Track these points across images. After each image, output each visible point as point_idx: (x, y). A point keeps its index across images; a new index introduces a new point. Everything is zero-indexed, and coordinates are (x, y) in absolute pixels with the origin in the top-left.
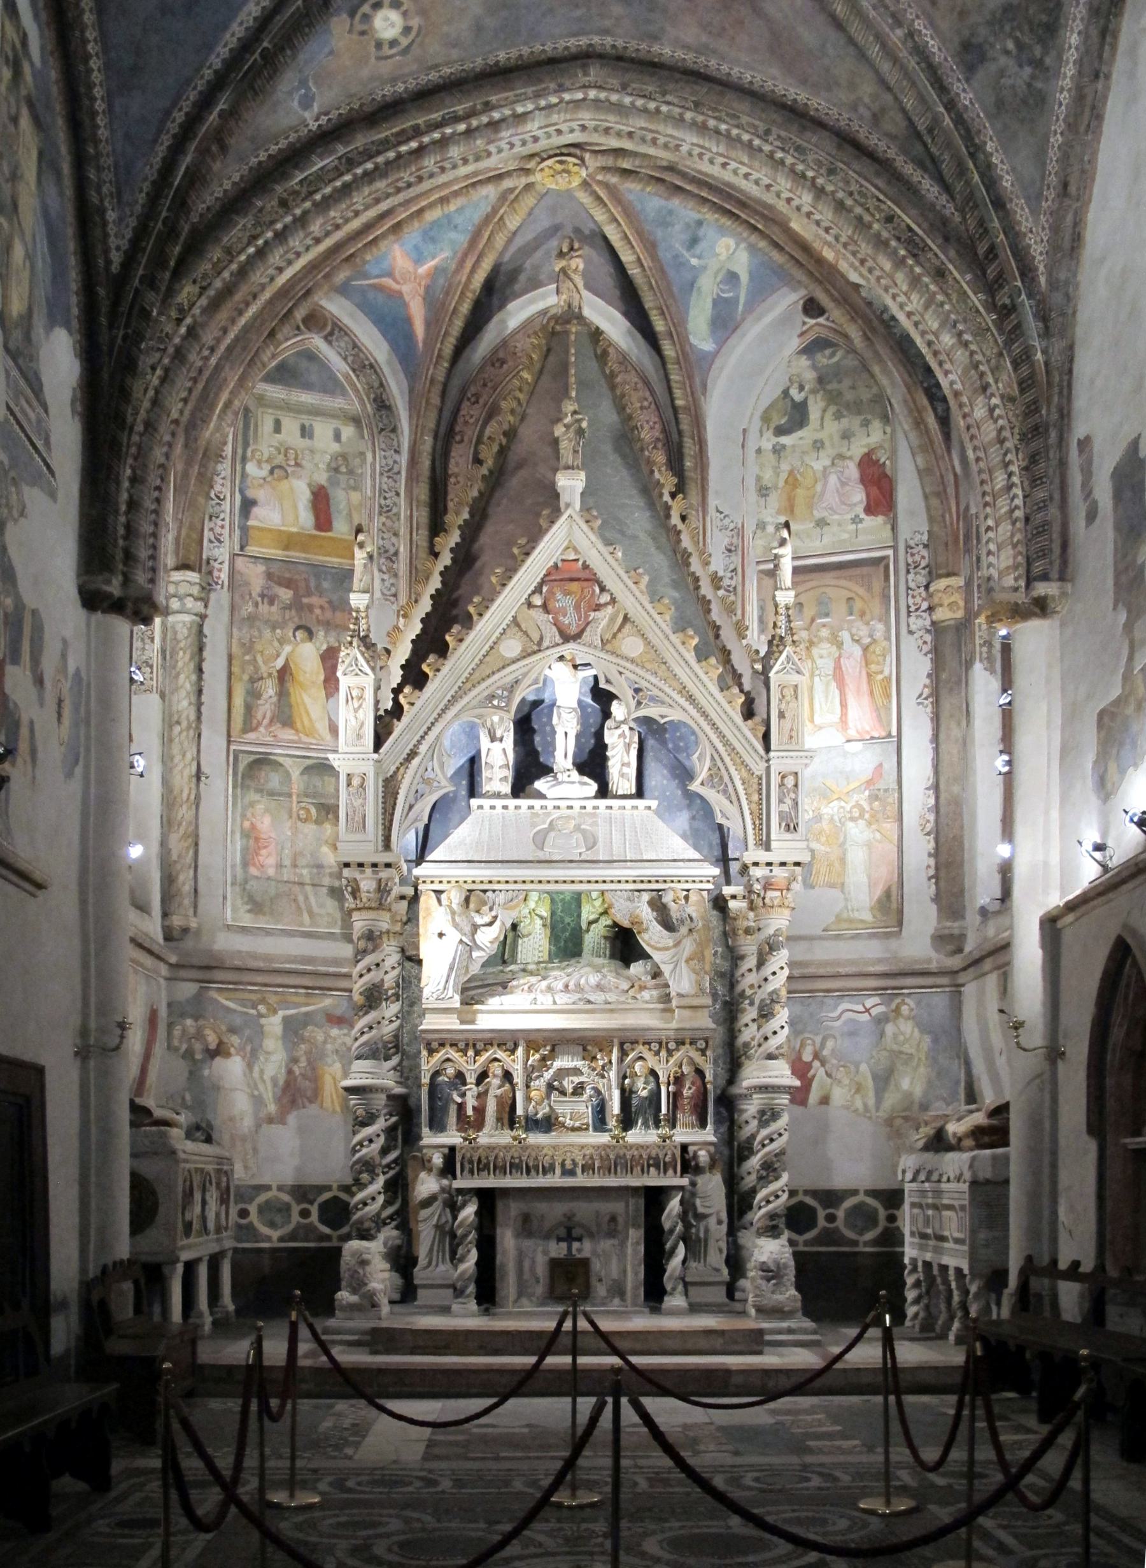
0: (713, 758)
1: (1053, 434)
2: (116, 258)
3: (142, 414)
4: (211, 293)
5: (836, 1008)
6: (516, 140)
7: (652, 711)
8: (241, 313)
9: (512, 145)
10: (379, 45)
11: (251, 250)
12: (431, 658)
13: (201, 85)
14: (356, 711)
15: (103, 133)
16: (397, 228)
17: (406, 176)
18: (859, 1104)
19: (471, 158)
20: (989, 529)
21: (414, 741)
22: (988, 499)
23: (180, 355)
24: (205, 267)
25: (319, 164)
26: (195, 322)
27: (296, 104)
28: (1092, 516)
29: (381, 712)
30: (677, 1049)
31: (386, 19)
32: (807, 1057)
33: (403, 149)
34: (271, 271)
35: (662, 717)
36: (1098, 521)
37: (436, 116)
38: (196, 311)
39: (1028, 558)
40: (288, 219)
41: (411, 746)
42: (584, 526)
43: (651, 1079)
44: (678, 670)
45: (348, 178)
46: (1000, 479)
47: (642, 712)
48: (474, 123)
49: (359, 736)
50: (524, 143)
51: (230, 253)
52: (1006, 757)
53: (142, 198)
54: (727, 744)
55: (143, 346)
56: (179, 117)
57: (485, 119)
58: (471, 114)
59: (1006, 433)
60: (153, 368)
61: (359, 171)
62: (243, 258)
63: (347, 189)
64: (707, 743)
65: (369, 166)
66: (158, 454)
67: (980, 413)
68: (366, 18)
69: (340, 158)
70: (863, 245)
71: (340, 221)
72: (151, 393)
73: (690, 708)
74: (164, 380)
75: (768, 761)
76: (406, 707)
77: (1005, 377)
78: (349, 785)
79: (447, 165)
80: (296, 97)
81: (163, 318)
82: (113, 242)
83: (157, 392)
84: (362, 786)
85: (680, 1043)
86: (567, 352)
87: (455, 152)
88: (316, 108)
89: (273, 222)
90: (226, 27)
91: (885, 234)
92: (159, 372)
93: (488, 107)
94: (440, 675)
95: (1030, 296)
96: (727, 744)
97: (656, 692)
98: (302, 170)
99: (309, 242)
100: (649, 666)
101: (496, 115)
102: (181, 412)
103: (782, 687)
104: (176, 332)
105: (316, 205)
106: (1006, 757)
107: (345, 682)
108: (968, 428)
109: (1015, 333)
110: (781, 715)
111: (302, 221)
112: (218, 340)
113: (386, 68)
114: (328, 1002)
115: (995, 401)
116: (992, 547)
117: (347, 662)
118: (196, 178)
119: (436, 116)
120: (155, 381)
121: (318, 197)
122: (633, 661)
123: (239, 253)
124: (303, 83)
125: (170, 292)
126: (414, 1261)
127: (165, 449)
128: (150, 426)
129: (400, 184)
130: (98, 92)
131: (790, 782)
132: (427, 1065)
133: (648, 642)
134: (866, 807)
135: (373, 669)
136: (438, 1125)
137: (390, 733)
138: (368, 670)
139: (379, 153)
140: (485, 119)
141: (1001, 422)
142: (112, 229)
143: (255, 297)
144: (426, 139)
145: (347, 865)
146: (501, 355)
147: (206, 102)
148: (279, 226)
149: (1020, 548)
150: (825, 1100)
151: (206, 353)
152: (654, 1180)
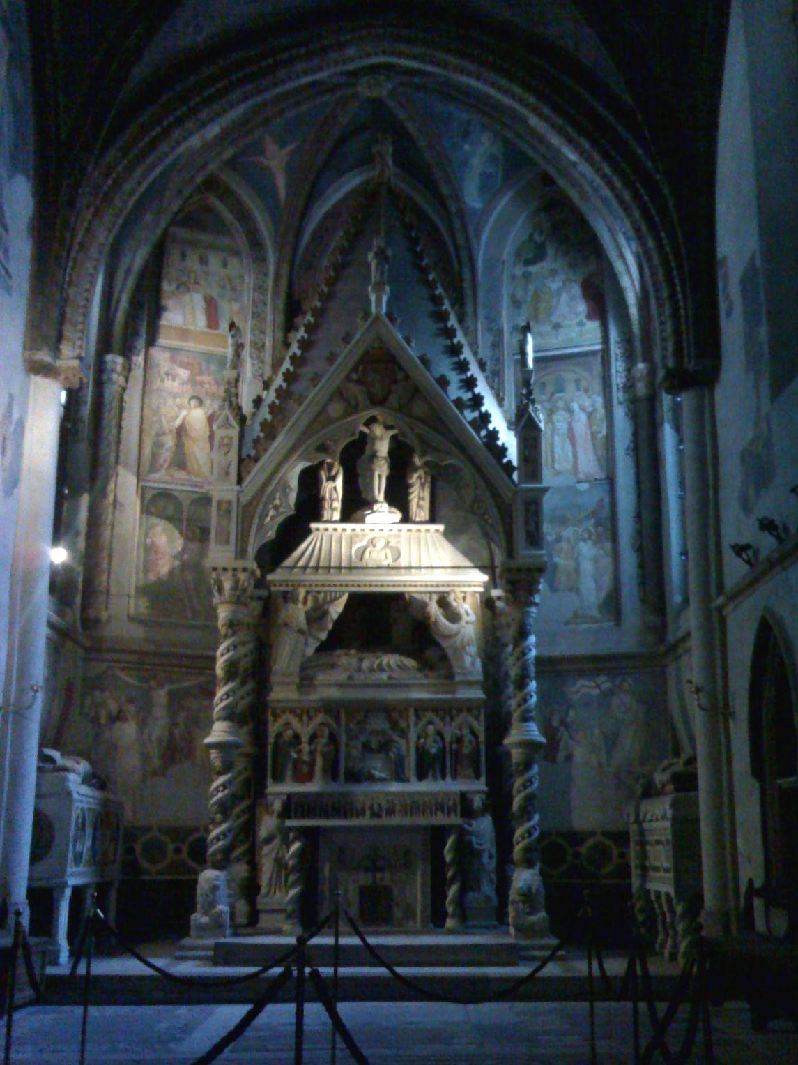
5: (574, 684)
14: (226, 454)
18: (594, 760)
25: (206, 71)
30: (458, 715)
32: (555, 723)
38: (120, 169)
43: (438, 738)
78: (219, 509)
83: (90, 223)
84: (229, 512)
85: (460, 710)
87: (299, 67)
102: (107, 238)
111: (194, 111)
114: (202, 679)
120: (89, 217)
126: (258, 888)
131: (533, 508)
132: (273, 728)
134: (593, 531)
136: (278, 778)
145: (215, 569)
150: (569, 758)
151: (126, 198)
152: (440, 819)
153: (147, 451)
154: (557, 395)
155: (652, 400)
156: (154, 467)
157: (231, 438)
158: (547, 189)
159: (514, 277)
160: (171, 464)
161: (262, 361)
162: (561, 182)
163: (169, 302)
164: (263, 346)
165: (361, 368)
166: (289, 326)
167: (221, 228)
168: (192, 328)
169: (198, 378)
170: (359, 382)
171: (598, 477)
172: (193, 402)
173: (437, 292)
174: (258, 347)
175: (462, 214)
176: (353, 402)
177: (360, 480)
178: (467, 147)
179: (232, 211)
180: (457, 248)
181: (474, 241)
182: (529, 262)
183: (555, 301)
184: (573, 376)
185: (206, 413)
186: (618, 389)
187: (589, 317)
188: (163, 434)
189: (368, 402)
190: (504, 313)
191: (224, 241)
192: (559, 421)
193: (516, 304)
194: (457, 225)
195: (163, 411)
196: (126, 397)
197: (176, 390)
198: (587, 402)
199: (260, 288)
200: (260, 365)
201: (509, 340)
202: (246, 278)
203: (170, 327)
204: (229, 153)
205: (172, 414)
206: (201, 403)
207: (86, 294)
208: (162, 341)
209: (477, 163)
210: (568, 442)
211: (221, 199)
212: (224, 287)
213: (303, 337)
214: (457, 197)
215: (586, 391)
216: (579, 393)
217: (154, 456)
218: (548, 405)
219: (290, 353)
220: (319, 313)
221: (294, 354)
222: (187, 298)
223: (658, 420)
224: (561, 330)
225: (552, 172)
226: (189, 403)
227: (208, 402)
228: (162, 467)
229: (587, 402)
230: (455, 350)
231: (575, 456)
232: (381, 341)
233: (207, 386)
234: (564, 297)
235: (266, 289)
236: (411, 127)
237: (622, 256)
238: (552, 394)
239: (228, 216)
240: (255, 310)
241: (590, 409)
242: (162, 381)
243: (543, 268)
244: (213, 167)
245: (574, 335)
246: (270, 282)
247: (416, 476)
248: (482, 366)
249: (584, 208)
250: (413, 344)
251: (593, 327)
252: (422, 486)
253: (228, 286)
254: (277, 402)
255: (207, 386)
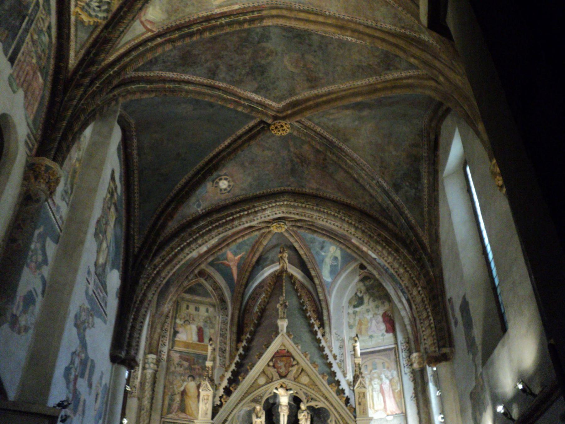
0: (335, 421)
1: (440, 298)
2: (136, 250)
3: (140, 298)
4: (166, 261)
6: (263, 216)
7: (313, 404)
8: (174, 267)
9: (261, 218)
10: (221, 190)
11: (179, 248)
12: (233, 385)
13: (167, 200)
14: (206, 404)
15: (136, 214)
16: (228, 245)
17: (228, 227)
19: (249, 222)
20: (423, 331)
21: (226, 416)
22: (422, 321)
23: (154, 280)
24: (164, 253)
25: (202, 223)
26: (159, 270)
27: (195, 206)
28: (456, 323)
29: (215, 405)
31: (223, 183)
33: (228, 219)
34: (185, 255)
35: (317, 406)
36: (458, 326)
37: (238, 210)
38: (160, 266)
39: (438, 341)
40: (191, 239)
41: (225, 418)
42: (287, 338)
44: (322, 389)
45: (210, 227)
46: (425, 315)
47: (309, 404)
48: (250, 211)
49: (206, 414)
50: (265, 217)
51: (172, 249)
52: (442, 416)
53: (146, 232)
54: (340, 415)
55: (142, 276)
56: (160, 209)
57: (253, 210)
58: (249, 209)
59: (425, 299)
60: (144, 284)
61: (214, 225)
62: (176, 251)
63: (210, 231)
64: (333, 415)
65: (217, 224)
66: (143, 311)
67: (415, 293)
68: (217, 183)
69: (208, 222)
70: (372, 243)
71: (207, 240)
72: (143, 291)
73: (326, 402)
74: (148, 287)
75: (356, 422)
76: (224, 403)
77: (422, 281)
79: (241, 223)
80: (196, 205)
81: (149, 268)
82: (136, 245)
83: (145, 291)
86: (282, 281)
87: (244, 220)
88: (202, 208)
89: (186, 240)
90: (176, 184)
91: (378, 239)
92: (146, 285)
93: (254, 207)
94: (237, 391)
95: (425, 254)
96: (340, 415)
97: (313, 396)
98: (197, 225)
99: (197, 246)
100: (311, 387)
101: (256, 209)
102: (152, 298)
103: (359, 393)
104: (153, 272)
105: (200, 235)
106: (442, 416)
107: (202, 393)
108: (412, 298)
109: (423, 267)
110: (359, 404)
111: (196, 240)
112: (166, 275)
113: (223, 197)
115: (420, 289)
116: (425, 337)
117: (204, 386)
118: (164, 226)
119: (238, 210)
120: (145, 288)
121: (201, 233)
122: (305, 385)
123: (175, 249)
124: (198, 201)
125: (152, 260)
127: (145, 309)
128: (142, 302)
129: (227, 229)
130: (137, 203)
133: (310, 378)
135: (213, 388)
137: (217, 413)
138: (210, 388)
139: (221, 220)
140: (253, 210)
141: (423, 295)
142: (136, 241)
143: (179, 262)
144: (235, 216)
146: (262, 284)
147: (168, 205)
148: (188, 241)
149: (435, 337)
151: (162, 279)
153: (166, 403)
154: (373, 371)
155: (423, 371)
156: (169, 412)
157: (208, 396)
158: (362, 271)
159: (348, 314)
160: (177, 411)
161: (225, 358)
162: (369, 268)
163: (180, 329)
164: (225, 350)
165: (274, 360)
166: (239, 340)
167: (206, 294)
168: (191, 342)
169: (193, 366)
170: (274, 366)
171: (397, 412)
172: (190, 379)
173: (311, 322)
174: (223, 351)
175: (321, 285)
176: (270, 377)
177: (274, 418)
178: (323, 254)
179: (211, 286)
180: (320, 301)
181: (328, 297)
182: (355, 306)
183: (369, 325)
184: (382, 361)
185: (196, 384)
186: (404, 366)
187: (387, 331)
188: (175, 394)
189: (278, 377)
190: (345, 331)
191: (208, 300)
192: (375, 384)
193: (351, 327)
194: (319, 290)
195: (175, 383)
196: (157, 376)
197: (181, 373)
198: (389, 374)
199: (224, 323)
200: (224, 360)
201: (348, 345)
202: (218, 318)
203: (180, 342)
204: (210, 259)
205: (179, 384)
206: (194, 379)
207: (141, 324)
208: (176, 348)
209: (328, 261)
210: (380, 395)
211: (206, 280)
212: (206, 322)
213: (245, 345)
214: (319, 277)
215: (388, 368)
216: (385, 369)
217: (170, 405)
218: (368, 376)
219: (239, 353)
220: (253, 334)
221: (241, 353)
222: (188, 327)
223: (426, 380)
224: (373, 339)
225: (365, 264)
226: (188, 379)
227: (198, 378)
228: (173, 411)
229: (389, 374)
230: (322, 349)
231: (385, 402)
232: (283, 345)
233: (197, 370)
234: (374, 322)
235: (227, 323)
236: (296, 245)
237: (401, 301)
238: (371, 371)
239: (210, 288)
240: (221, 333)
241: (390, 377)
242: (175, 368)
243: (362, 309)
244: (203, 266)
245: (380, 341)
246: (229, 318)
247: (303, 414)
248: (335, 357)
249: (381, 280)
250: (300, 347)
251: (390, 335)
252: (306, 419)
253: (209, 322)
254: (232, 378)
255: (197, 370)
